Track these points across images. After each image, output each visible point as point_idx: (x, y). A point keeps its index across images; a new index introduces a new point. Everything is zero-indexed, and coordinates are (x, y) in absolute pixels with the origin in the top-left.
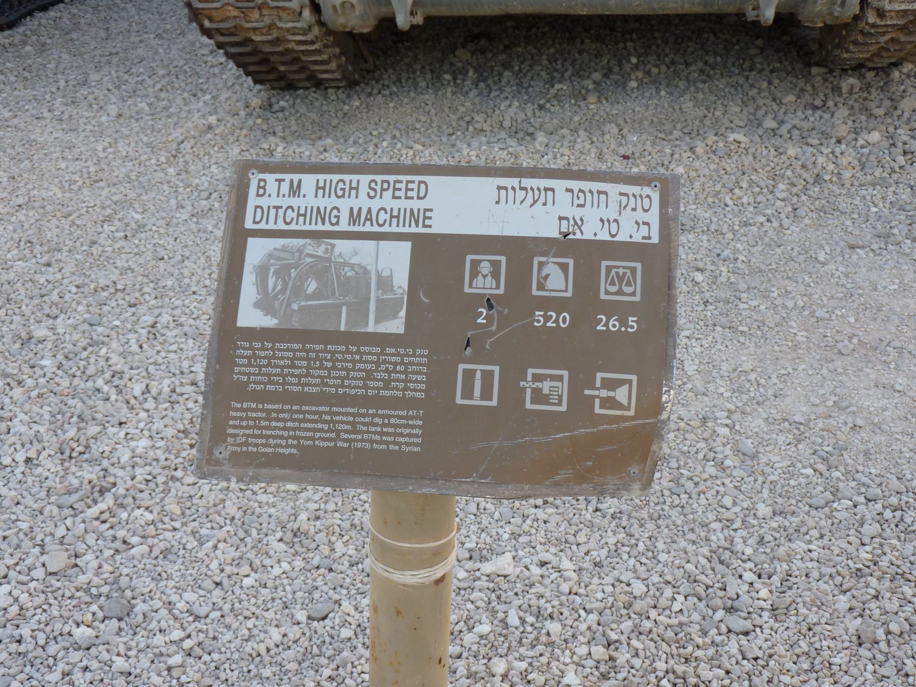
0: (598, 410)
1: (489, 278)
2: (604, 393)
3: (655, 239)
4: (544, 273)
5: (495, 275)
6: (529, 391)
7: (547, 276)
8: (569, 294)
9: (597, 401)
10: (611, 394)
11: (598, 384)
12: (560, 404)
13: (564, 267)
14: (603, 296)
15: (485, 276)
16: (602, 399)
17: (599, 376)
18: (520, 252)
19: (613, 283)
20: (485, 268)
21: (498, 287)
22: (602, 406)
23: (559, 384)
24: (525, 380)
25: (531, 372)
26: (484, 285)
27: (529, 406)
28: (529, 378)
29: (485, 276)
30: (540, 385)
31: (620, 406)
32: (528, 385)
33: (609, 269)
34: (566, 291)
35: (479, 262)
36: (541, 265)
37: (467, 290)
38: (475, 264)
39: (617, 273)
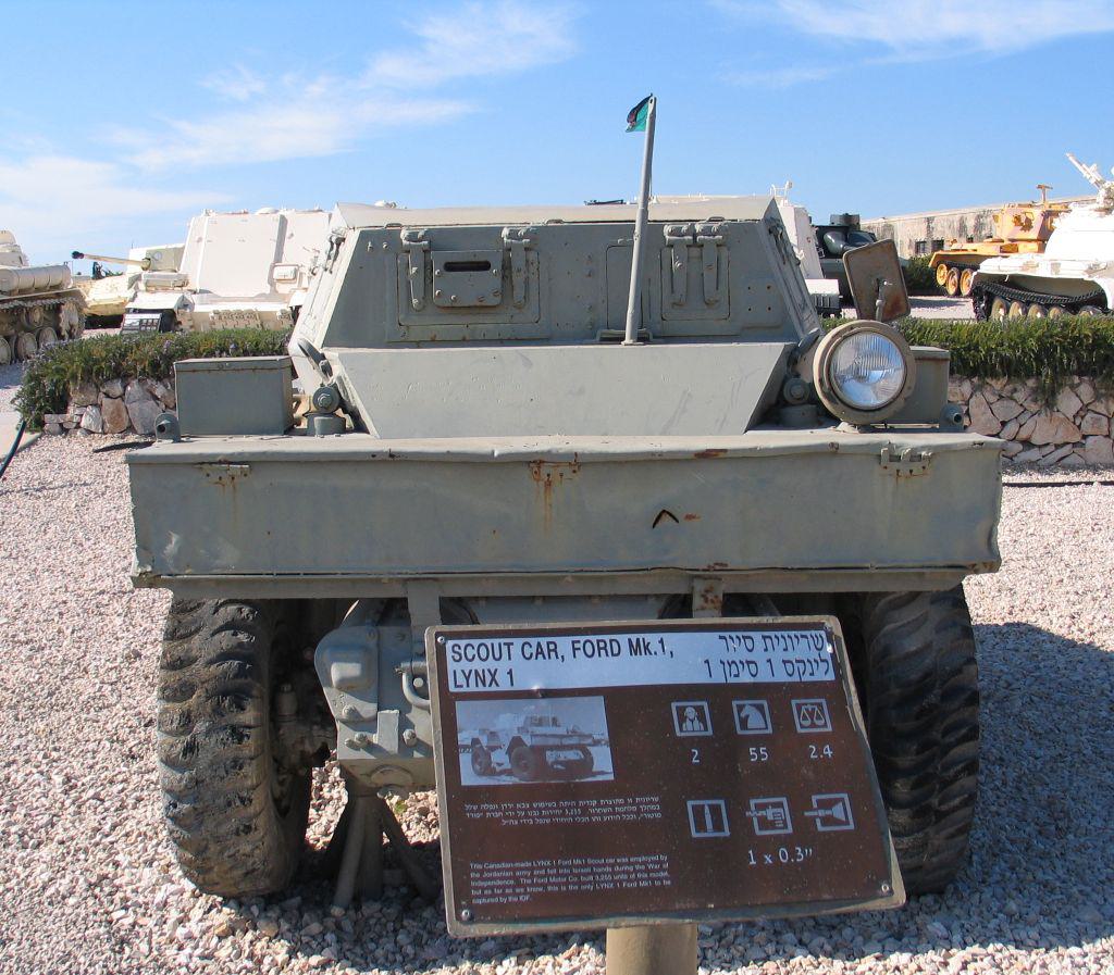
0: (820, 828)
1: (696, 722)
3: (831, 677)
4: (743, 715)
5: (701, 718)
6: (755, 820)
7: (747, 716)
8: (770, 731)
9: (818, 820)
10: (828, 812)
11: (815, 806)
12: (786, 827)
13: (760, 708)
14: (800, 730)
18: (719, 697)
19: (805, 718)
20: (691, 713)
21: (706, 729)
22: (823, 824)
24: (749, 809)
25: (752, 803)
27: (758, 832)
28: (753, 808)
30: (764, 813)
31: (838, 822)
32: (753, 814)
33: (799, 707)
34: (767, 728)
35: (684, 708)
36: (740, 708)
37: (678, 734)
38: (681, 710)
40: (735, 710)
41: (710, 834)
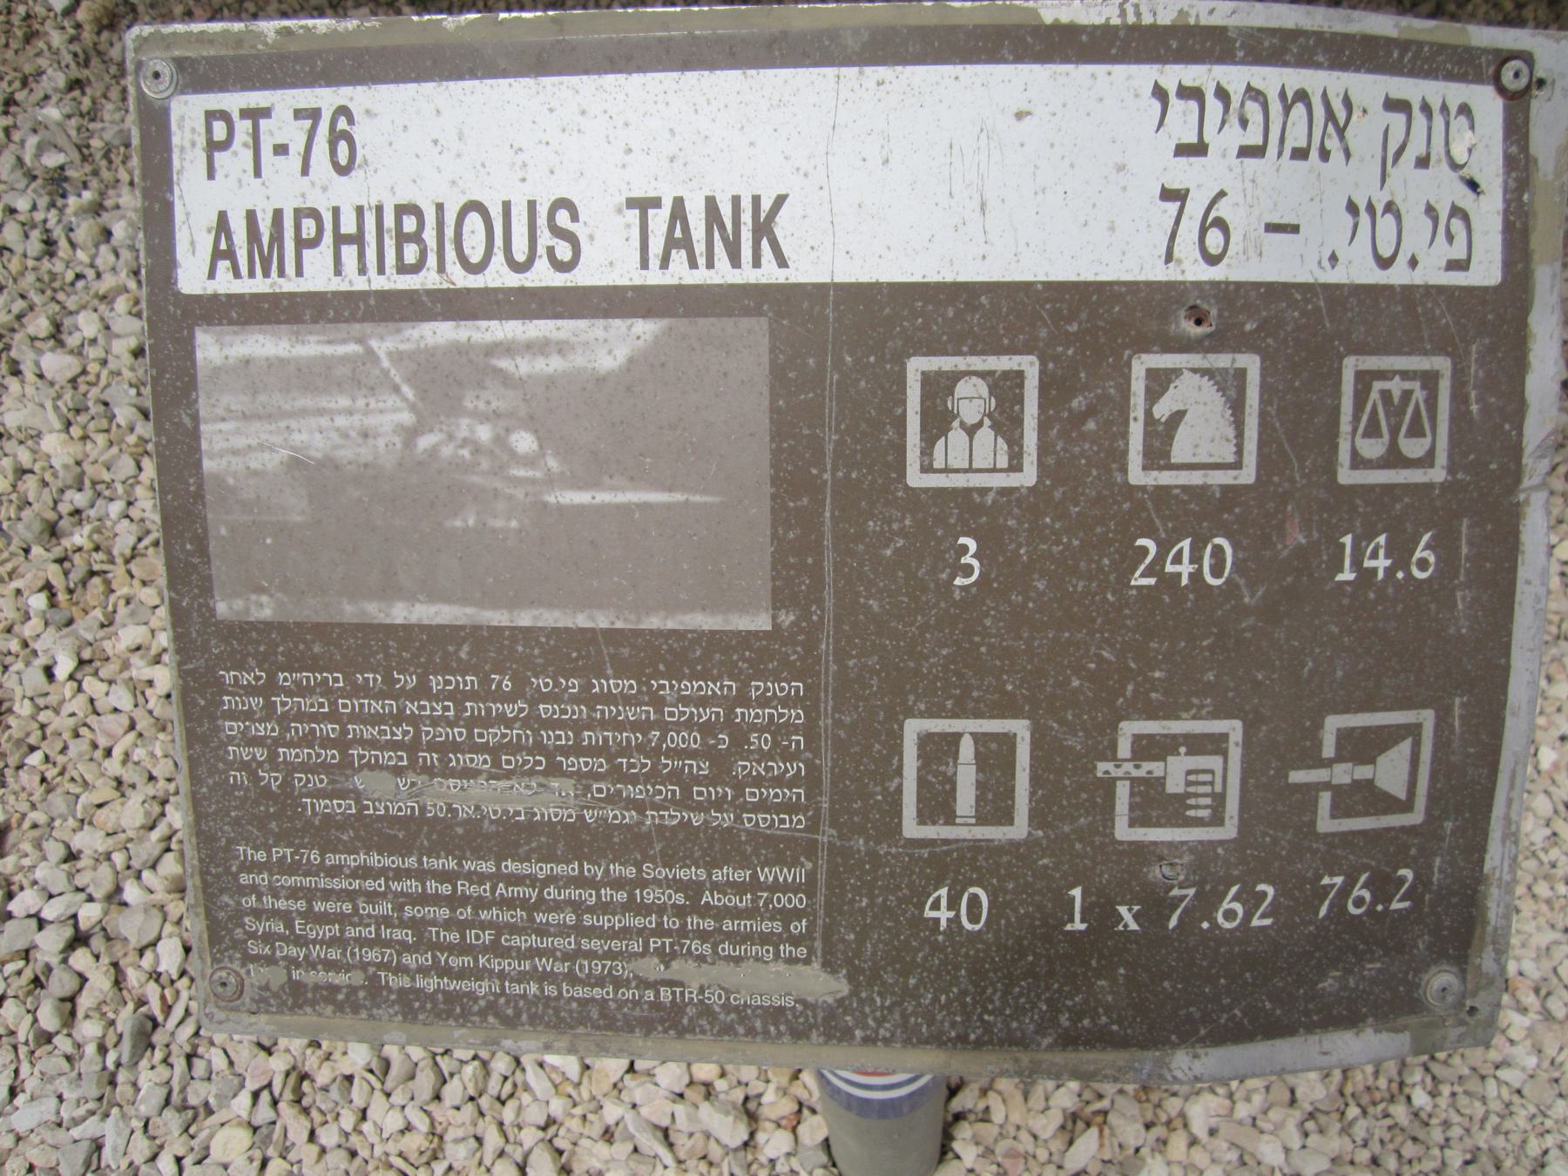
0: (1326, 823)
1: (986, 435)
2: (1343, 774)
3: (1487, 271)
4: (1162, 410)
5: (1006, 422)
6: (1123, 792)
9: (1325, 799)
10: (1364, 772)
11: (1328, 751)
12: (1217, 820)
15: (971, 431)
16: (1338, 791)
17: (1333, 723)
19: (1373, 431)
20: (971, 400)
21: (1015, 466)
22: (1338, 811)
23: (1214, 762)
24: (1114, 758)
26: (971, 459)
27: (1123, 831)
28: (1124, 749)
29: (971, 431)
30: (1156, 768)
31: (1389, 804)
32: (1120, 770)
37: (915, 478)
38: (938, 388)
39: (1386, 395)
40: (1138, 386)
41: (965, 830)
